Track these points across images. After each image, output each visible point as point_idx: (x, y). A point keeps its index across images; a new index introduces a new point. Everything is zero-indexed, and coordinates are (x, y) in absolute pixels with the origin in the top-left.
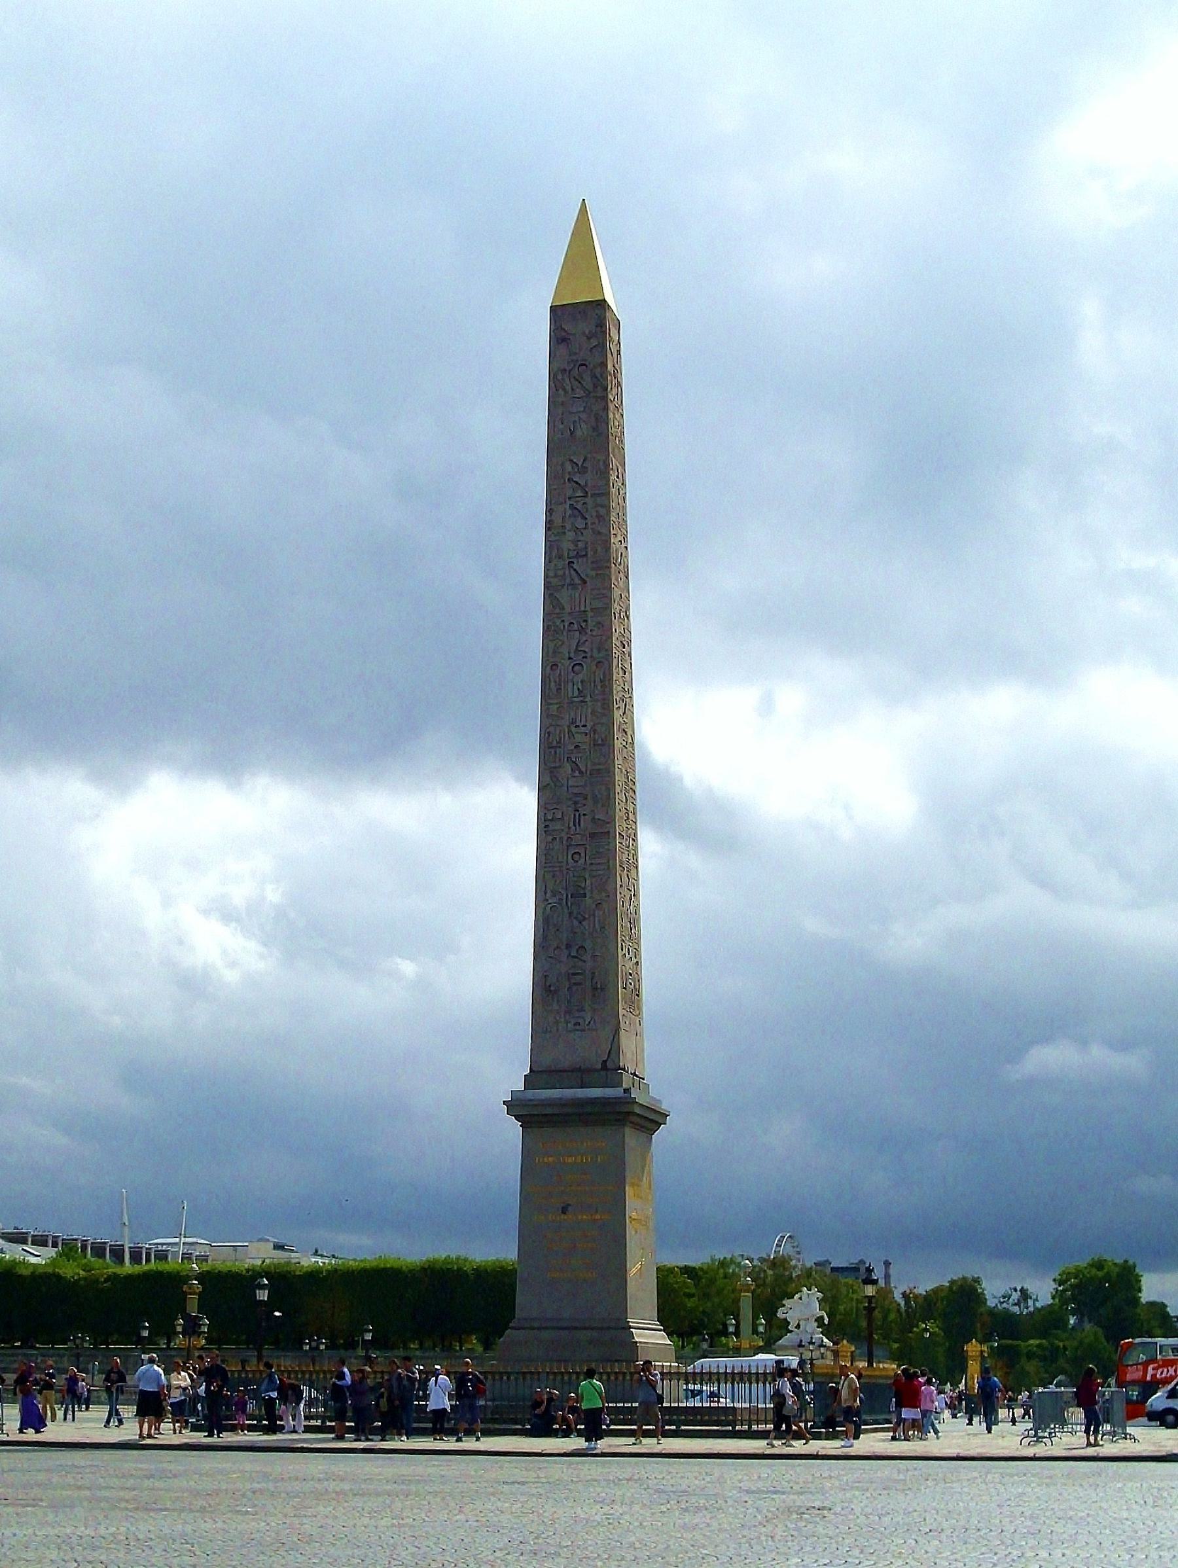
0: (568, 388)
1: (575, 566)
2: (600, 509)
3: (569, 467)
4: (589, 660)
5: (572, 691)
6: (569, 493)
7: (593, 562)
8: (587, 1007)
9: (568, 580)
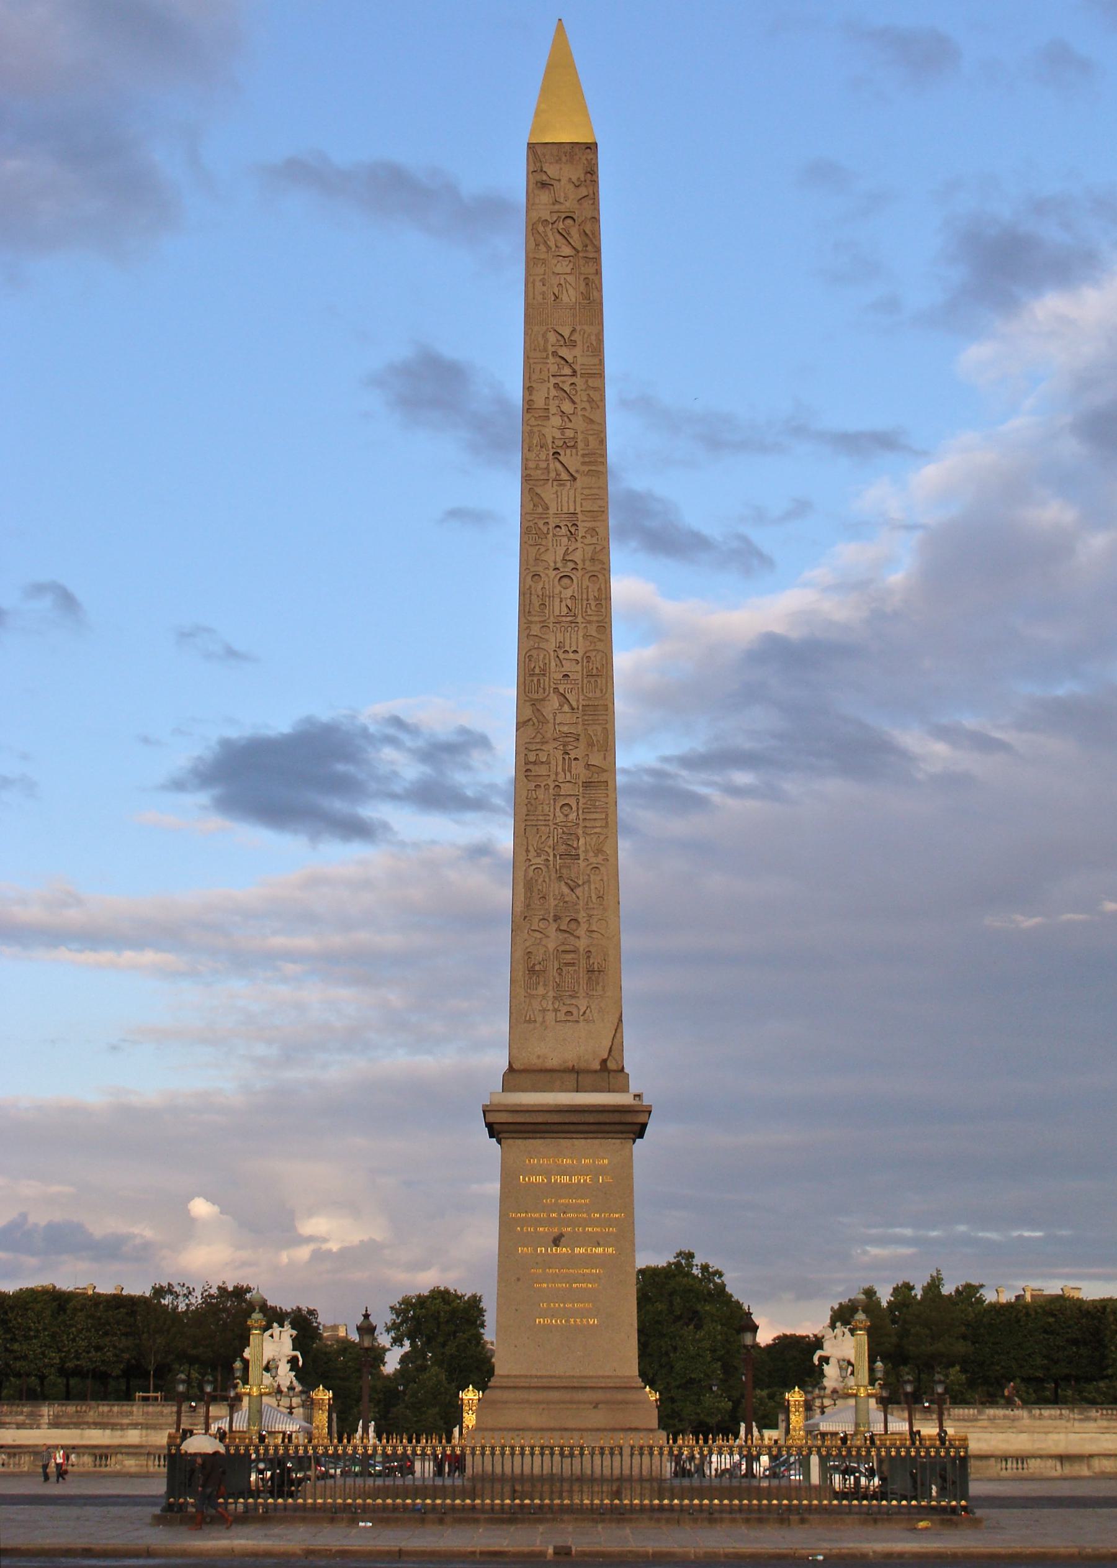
0: (552, 244)
1: (561, 458)
2: (591, 393)
3: (552, 338)
4: (580, 573)
5: (559, 608)
6: (554, 369)
7: (583, 456)
8: (581, 994)
9: (553, 475)
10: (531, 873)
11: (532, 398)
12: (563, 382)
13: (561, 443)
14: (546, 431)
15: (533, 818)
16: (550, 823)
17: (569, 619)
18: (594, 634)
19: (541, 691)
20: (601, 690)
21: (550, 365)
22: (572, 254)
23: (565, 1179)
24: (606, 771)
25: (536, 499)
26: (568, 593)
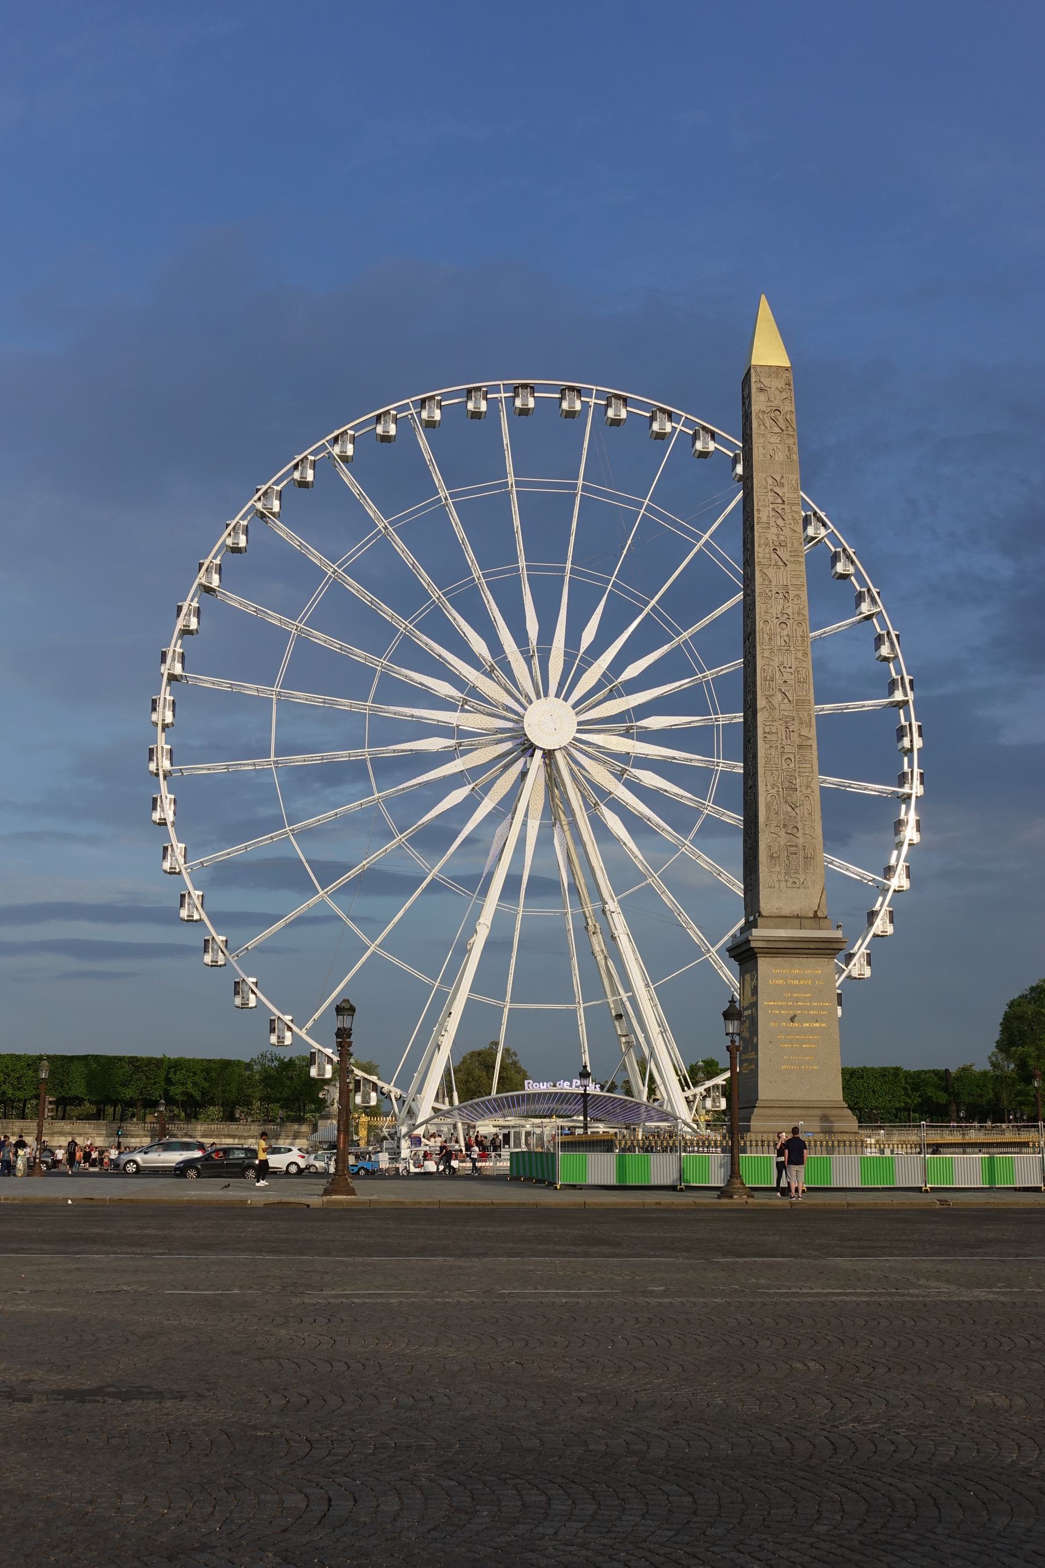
0: (768, 425)
1: (778, 553)
2: (794, 514)
3: (770, 481)
4: (791, 621)
5: (779, 641)
6: (771, 499)
7: (790, 551)
8: (801, 871)
9: (773, 562)
10: (769, 799)
11: (760, 516)
13: (777, 543)
14: (768, 536)
15: (768, 765)
16: (779, 769)
17: (786, 648)
18: (801, 658)
19: (771, 690)
20: (806, 691)
21: (769, 497)
23: (796, 982)
25: (764, 576)
26: (785, 632)
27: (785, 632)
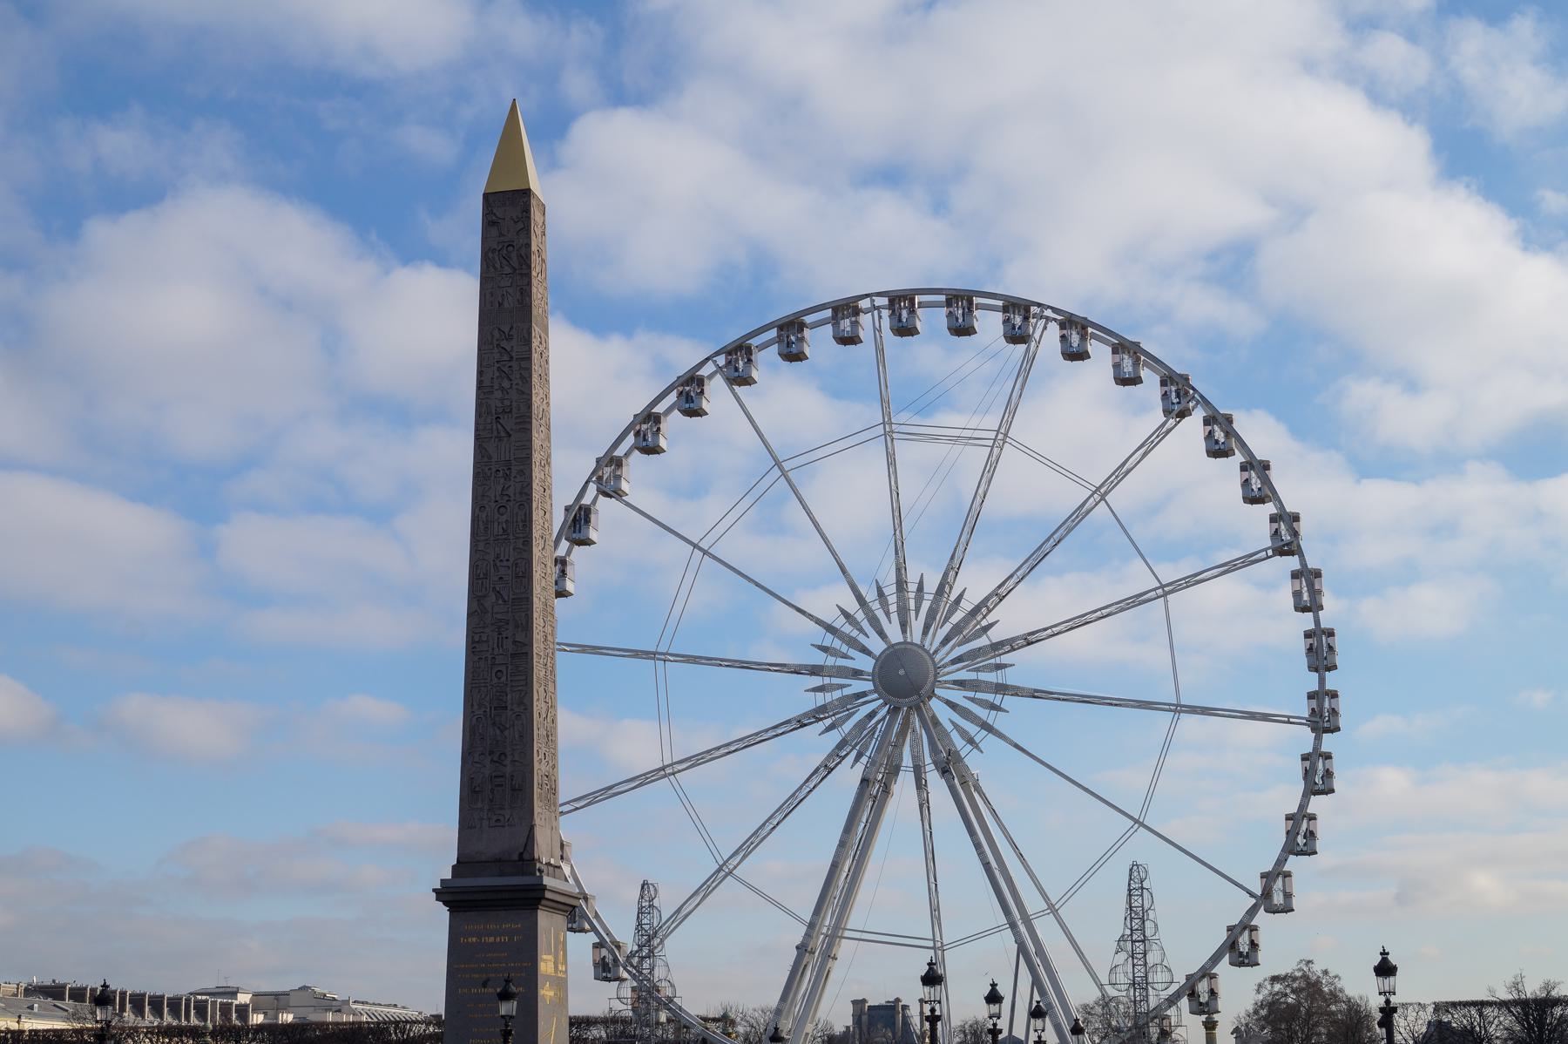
0: (498, 266)
3: (496, 333)
4: (511, 504)
6: (497, 356)
7: (516, 418)
9: (495, 433)
12: (505, 365)
13: (500, 410)
17: (504, 537)
18: (521, 546)
19: (484, 590)
22: (511, 272)
23: (492, 939)
24: (526, 645)
25: (484, 451)
26: (504, 518)
27: (504, 518)
